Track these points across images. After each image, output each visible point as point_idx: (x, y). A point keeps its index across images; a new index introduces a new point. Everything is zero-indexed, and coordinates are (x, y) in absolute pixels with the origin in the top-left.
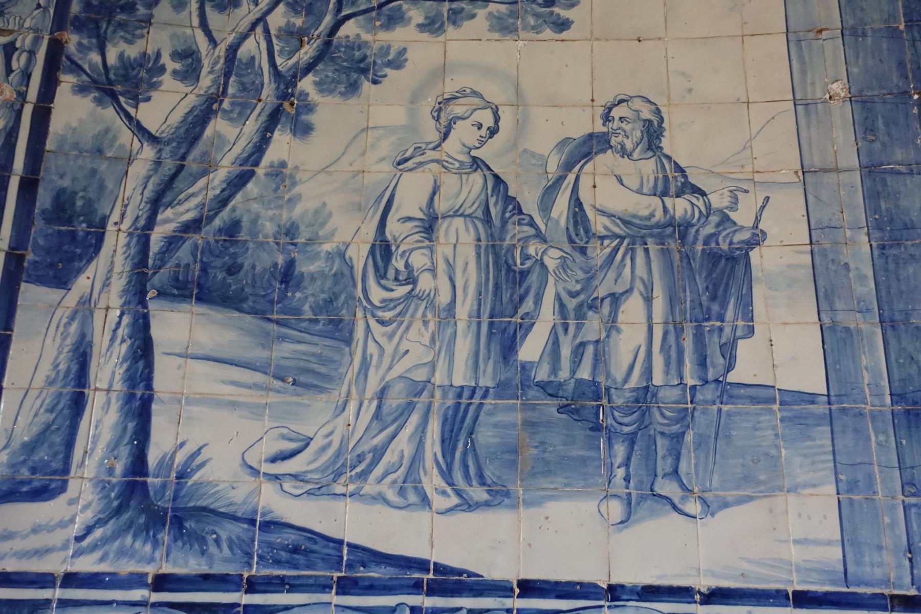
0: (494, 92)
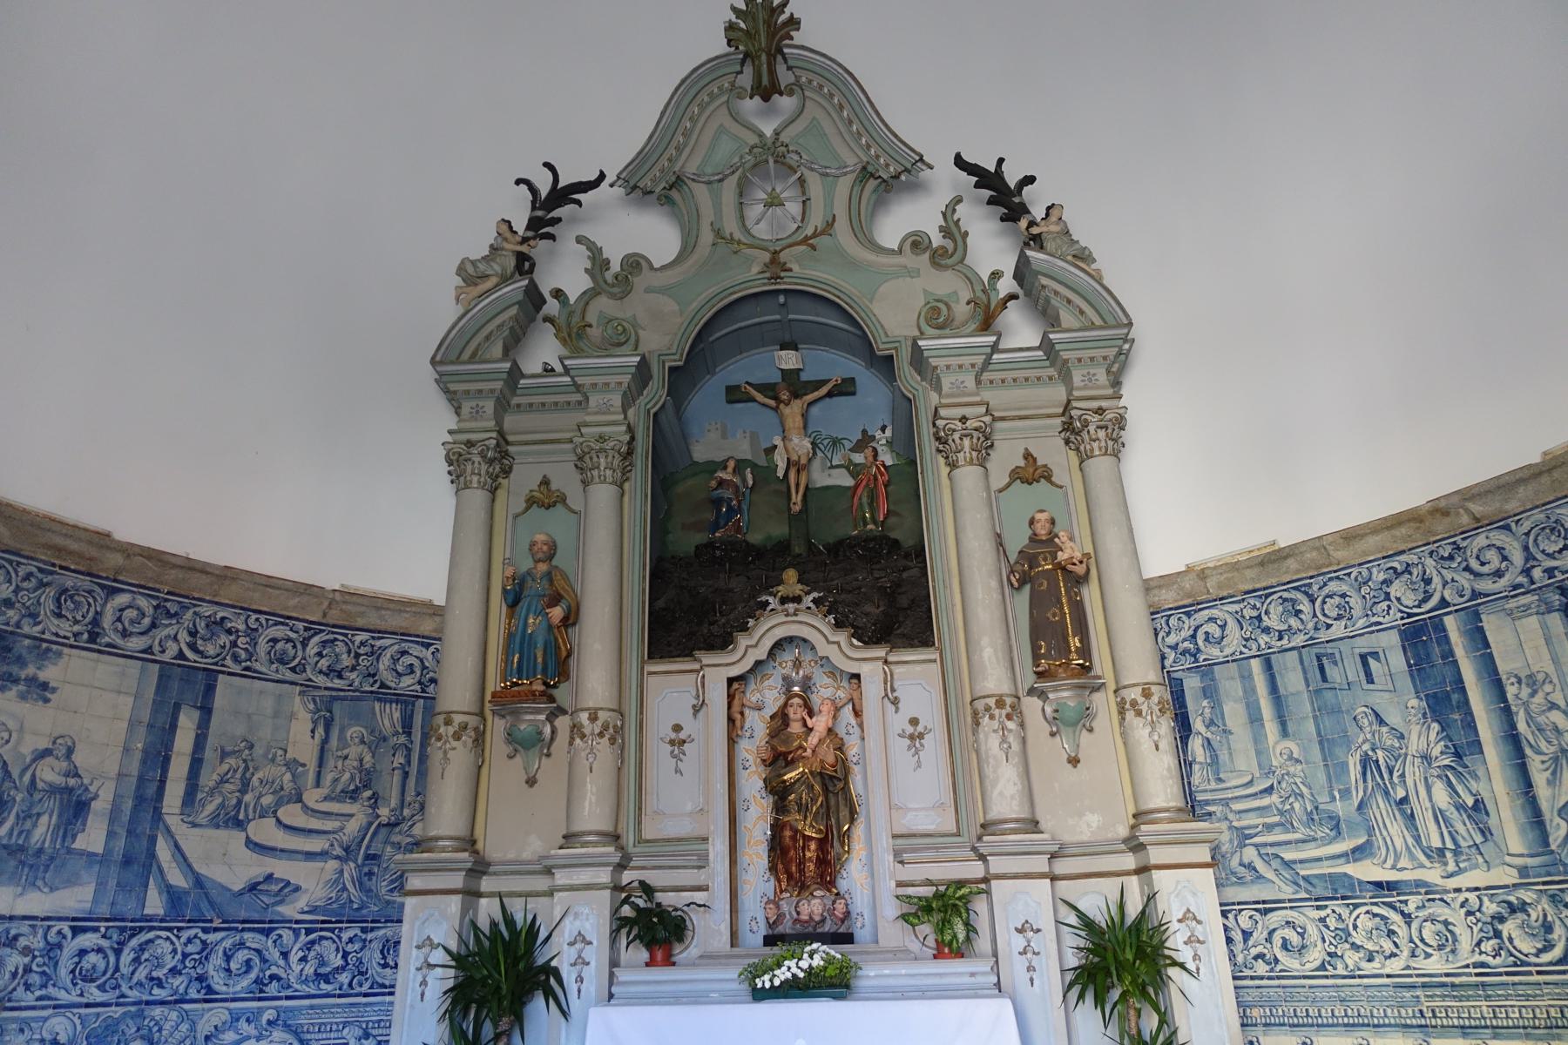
0: (11, 724)
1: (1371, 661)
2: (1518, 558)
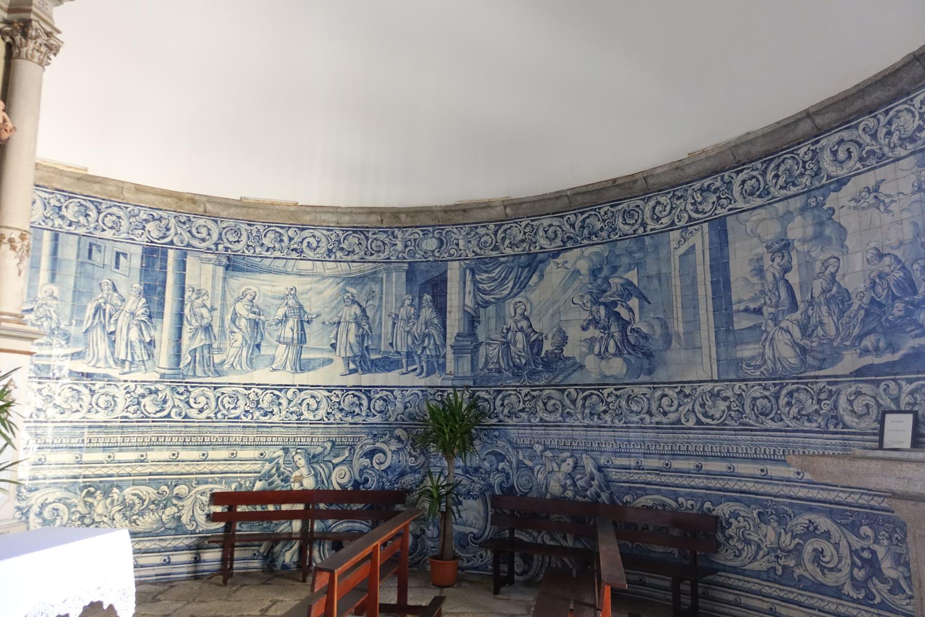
1: (122, 257)
2: (215, 237)
